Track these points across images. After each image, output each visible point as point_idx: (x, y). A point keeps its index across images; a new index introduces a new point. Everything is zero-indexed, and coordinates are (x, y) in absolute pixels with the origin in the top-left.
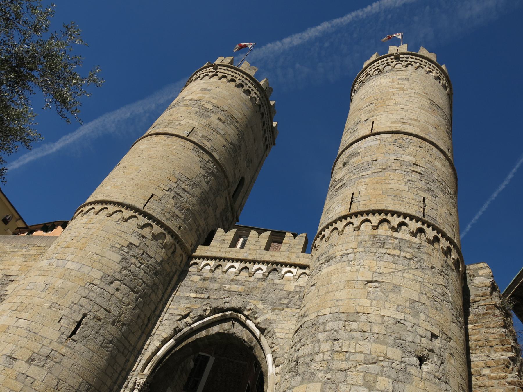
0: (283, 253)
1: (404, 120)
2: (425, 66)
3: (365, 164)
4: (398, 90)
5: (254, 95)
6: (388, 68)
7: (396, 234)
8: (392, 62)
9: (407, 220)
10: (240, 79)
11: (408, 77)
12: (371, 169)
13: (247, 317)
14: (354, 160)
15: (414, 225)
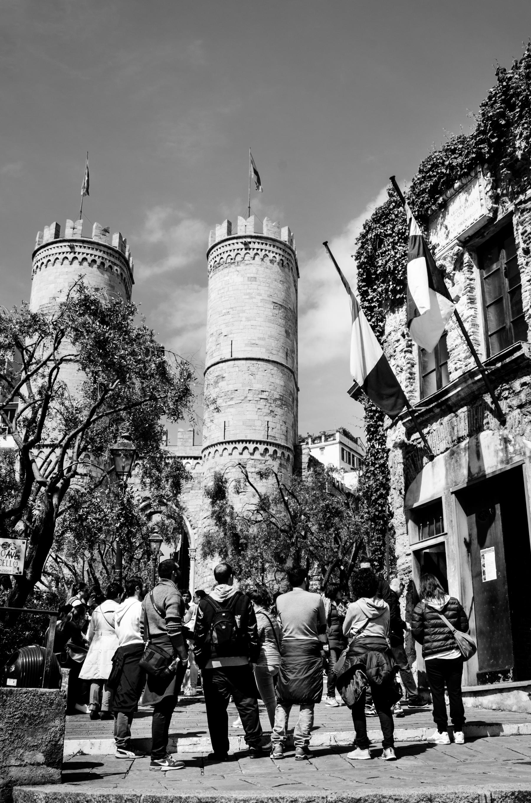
0: (180, 448)
1: (254, 342)
2: (269, 251)
3: (229, 393)
4: (247, 297)
5: (115, 268)
6: (239, 258)
7: (252, 457)
8: (242, 249)
9: (258, 445)
10: (99, 257)
11: (255, 276)
12: (234, 399)
13: (167, 500)
14: (222, 384)
15: (262, 448)
